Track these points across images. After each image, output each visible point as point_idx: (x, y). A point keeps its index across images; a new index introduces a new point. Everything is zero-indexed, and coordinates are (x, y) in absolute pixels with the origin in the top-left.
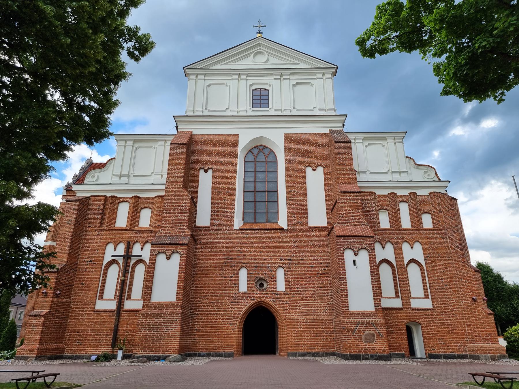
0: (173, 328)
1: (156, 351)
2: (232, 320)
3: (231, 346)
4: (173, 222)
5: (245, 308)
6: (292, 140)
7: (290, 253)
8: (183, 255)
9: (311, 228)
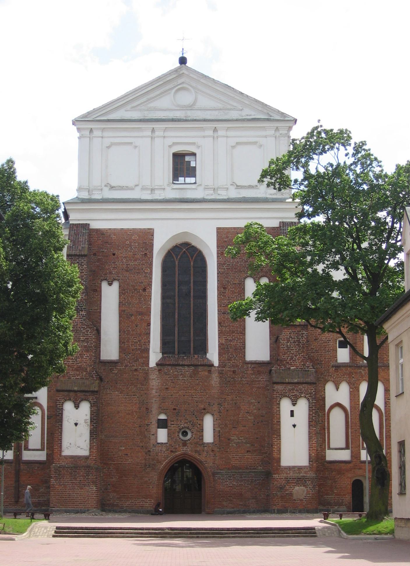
4: (77, 362)
8: (93, 403)
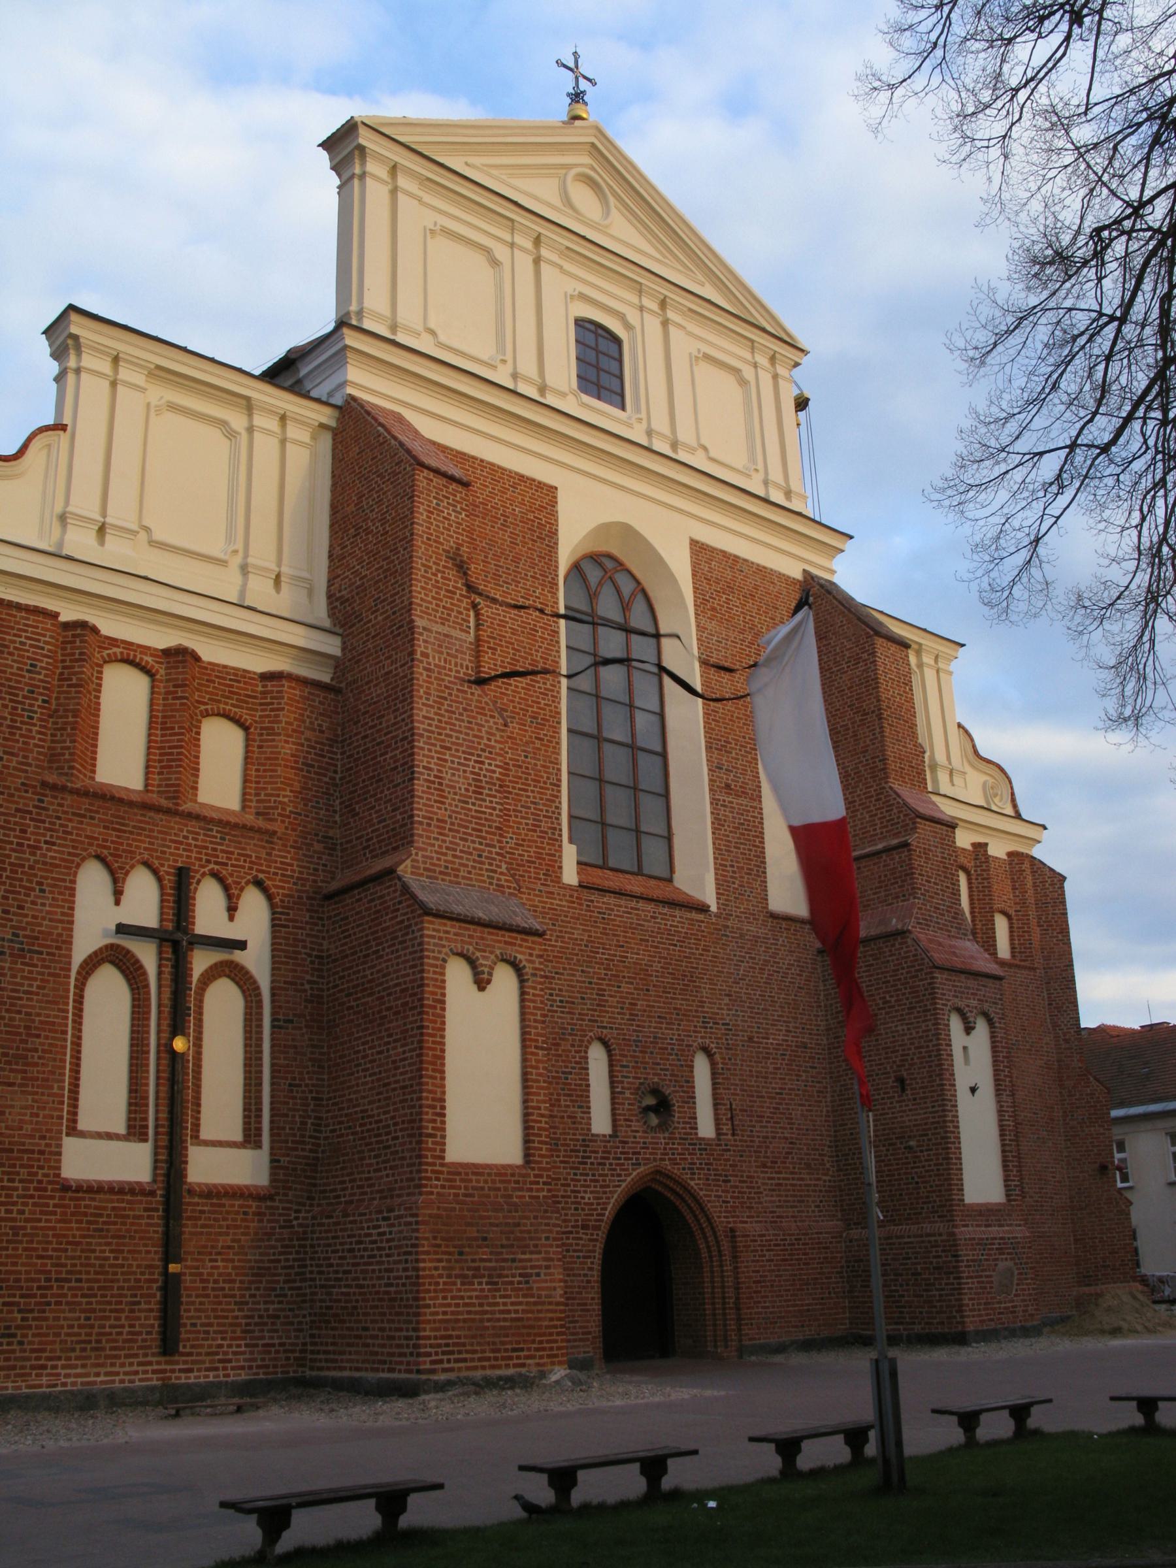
0: (540, 1267)
1: (496, 1359)
2: (581, 1239)
3: (583, 1334)
4: (452, 824)
5: (616, 1196)
6: (711, 570)
7: (726, 1000)
9: (774, 916)
